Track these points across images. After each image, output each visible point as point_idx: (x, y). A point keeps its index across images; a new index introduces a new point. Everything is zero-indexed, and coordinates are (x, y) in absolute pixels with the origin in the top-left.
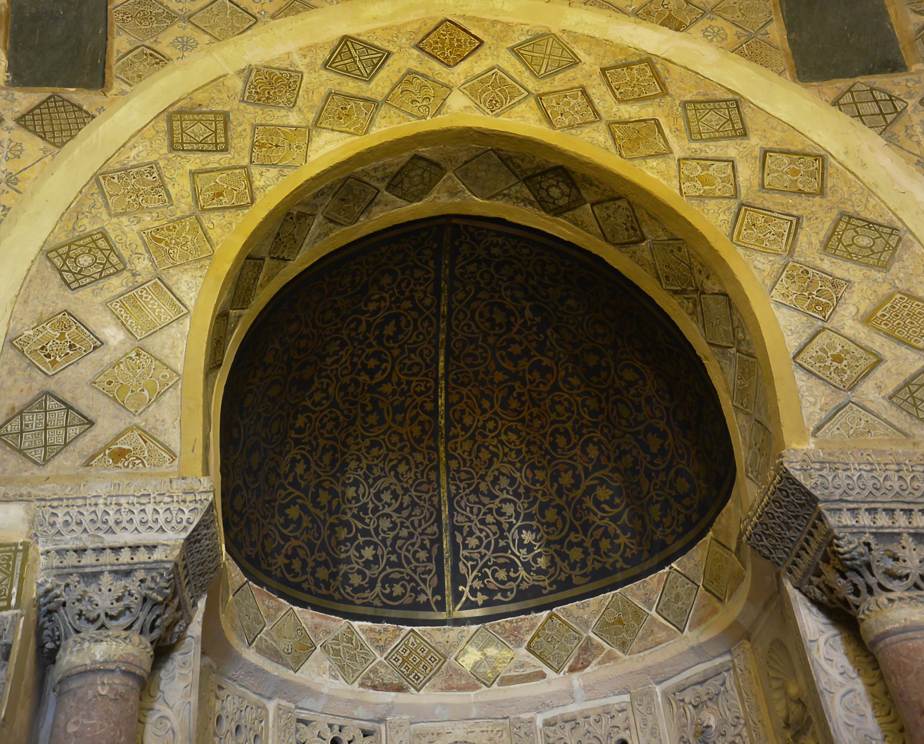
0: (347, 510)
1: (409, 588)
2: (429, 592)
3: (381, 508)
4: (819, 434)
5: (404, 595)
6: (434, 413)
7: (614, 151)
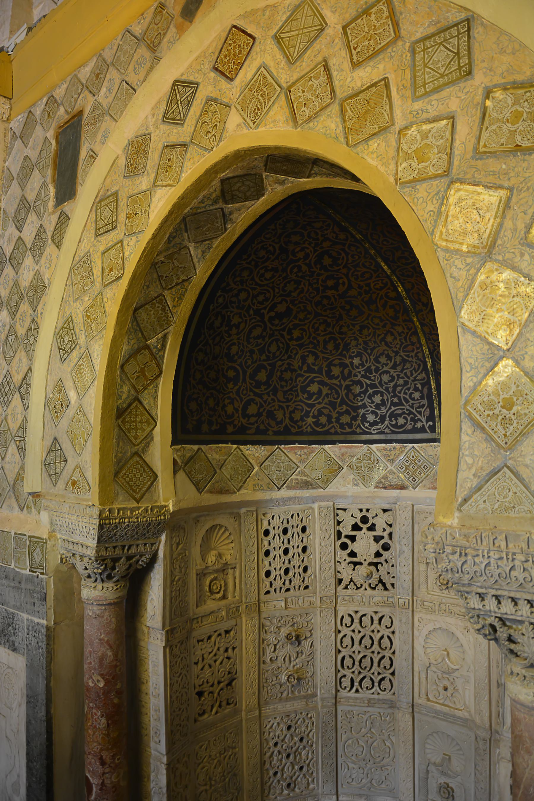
1: (409, 419)
2: (424, 420)
4: (465, 507)
5: (405, 424)
6: (399, 297)
7: (342, 139)
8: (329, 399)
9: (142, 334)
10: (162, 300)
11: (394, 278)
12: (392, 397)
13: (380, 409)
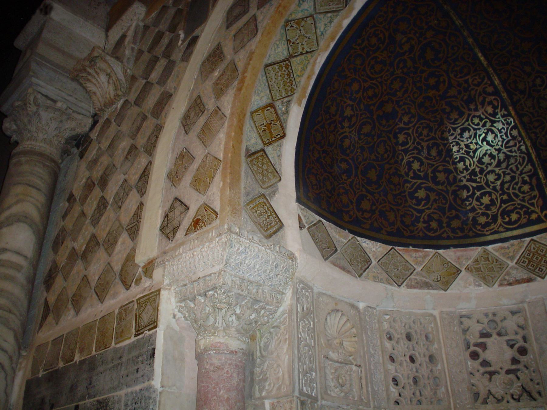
0: (462, 178)
1: (522, 213)
2: (538, 210)
3: (485, 168)
6: (496, 93)
8: (438, 204)
9: (270, 92)
10: (287, 64)
11: (490, 70)
12: (500, 195)
13: (490, 210)
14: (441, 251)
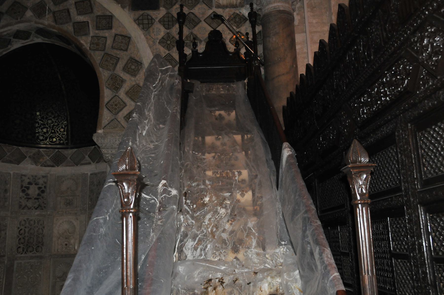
2: (64, 140)
14: (20, 148)
